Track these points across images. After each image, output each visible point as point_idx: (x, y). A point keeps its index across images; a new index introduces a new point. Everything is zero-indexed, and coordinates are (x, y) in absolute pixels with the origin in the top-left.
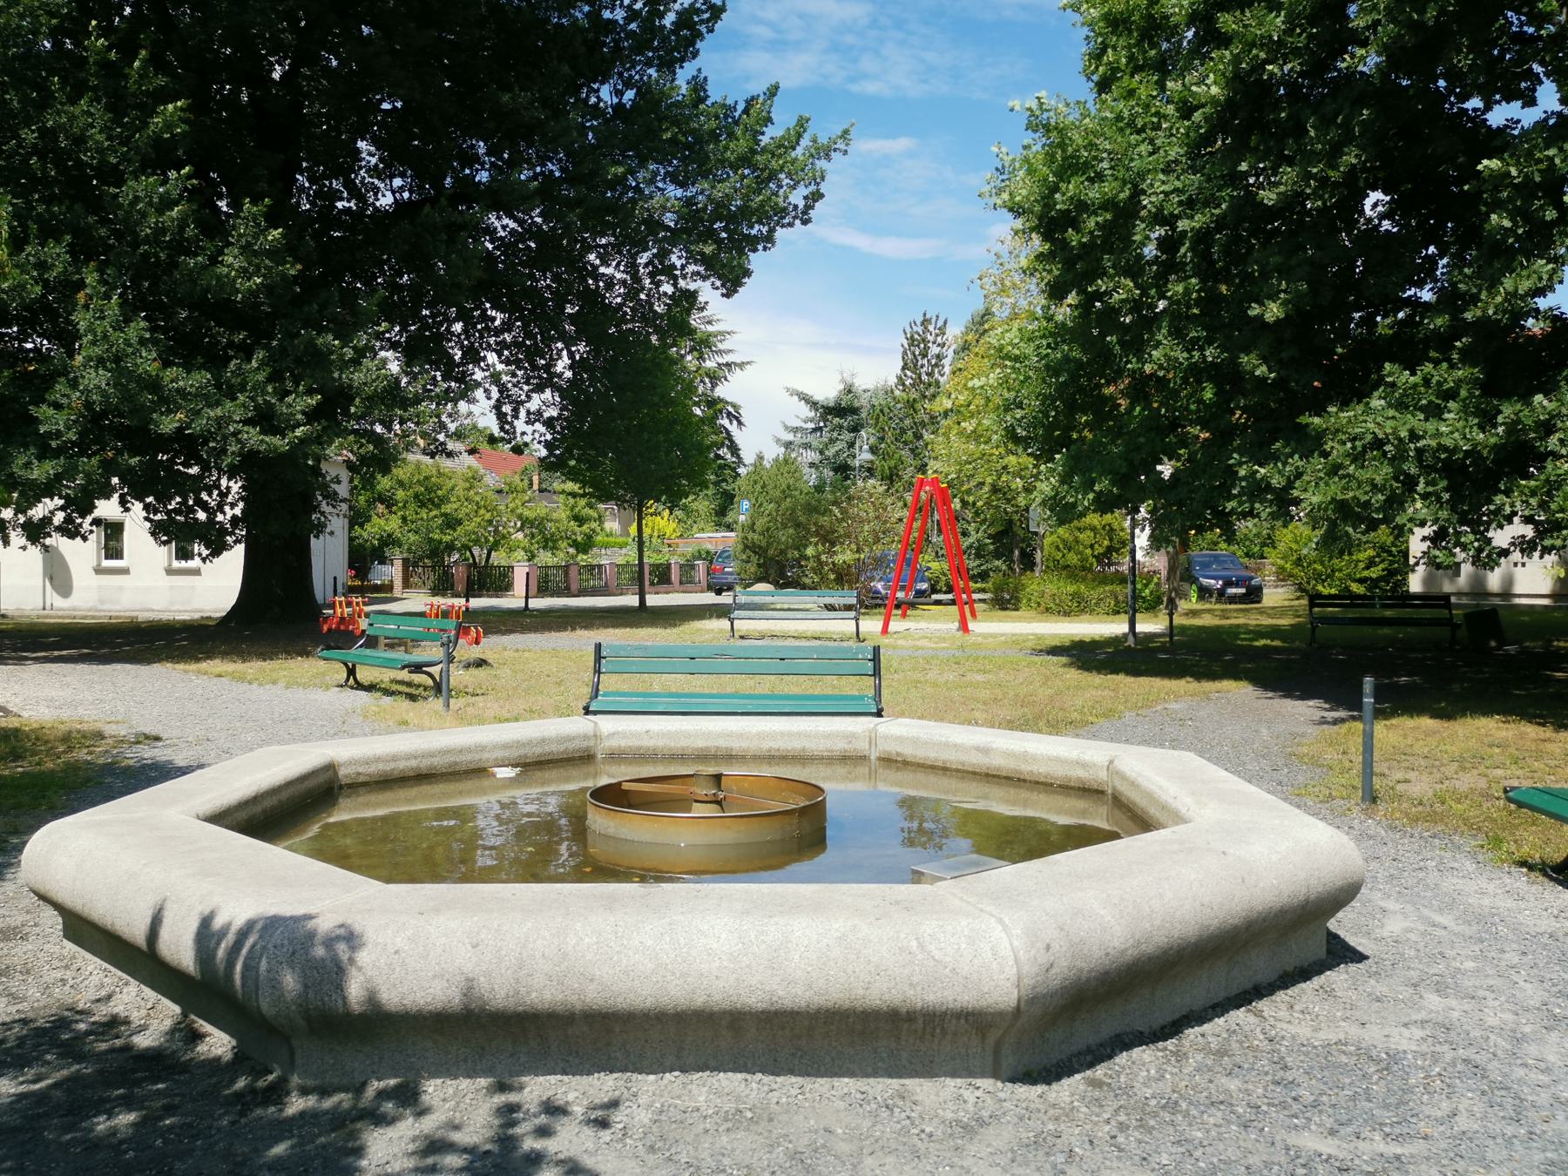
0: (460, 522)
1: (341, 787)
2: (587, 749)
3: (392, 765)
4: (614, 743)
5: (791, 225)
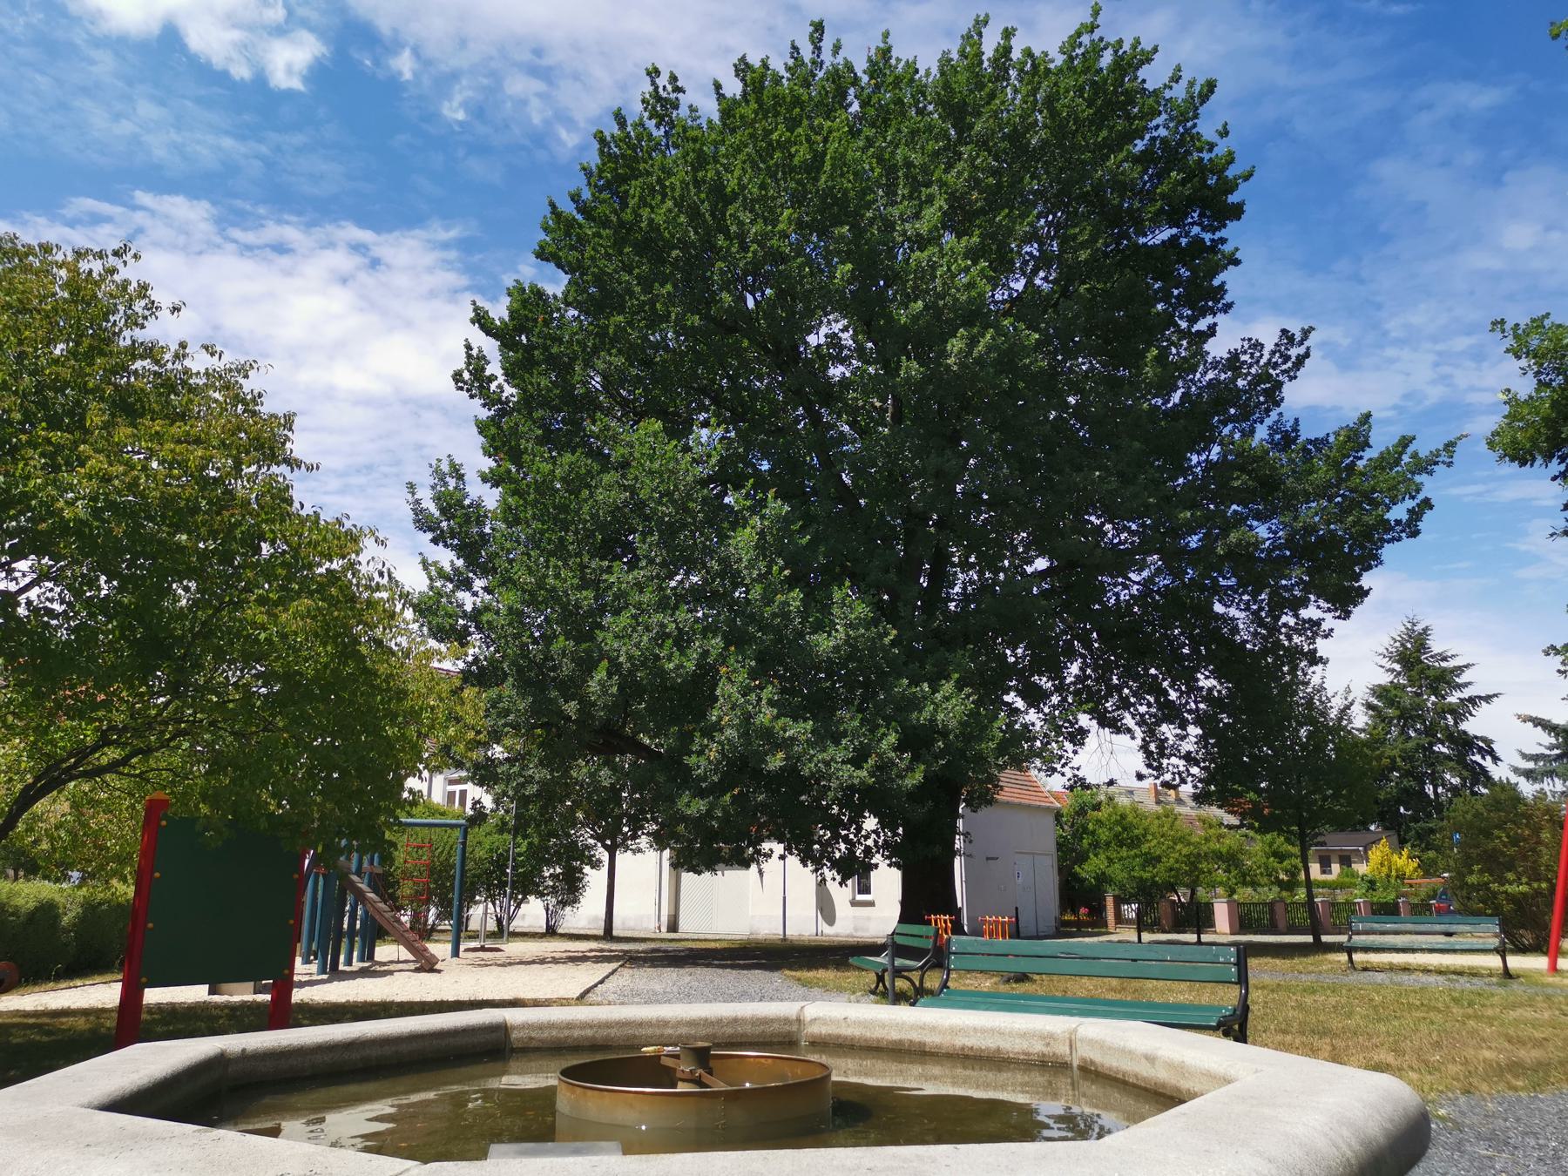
0: (1158, 859)
1: (513, 1050)
2: (789, 1033)
3: (566, 1033)
4: (815, 1030)
5: (1399, 539)
